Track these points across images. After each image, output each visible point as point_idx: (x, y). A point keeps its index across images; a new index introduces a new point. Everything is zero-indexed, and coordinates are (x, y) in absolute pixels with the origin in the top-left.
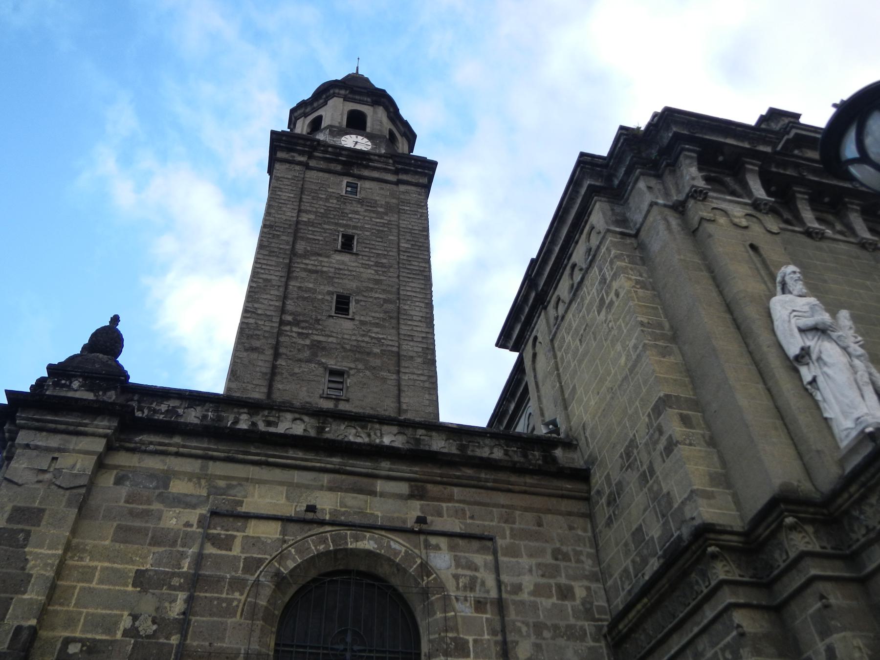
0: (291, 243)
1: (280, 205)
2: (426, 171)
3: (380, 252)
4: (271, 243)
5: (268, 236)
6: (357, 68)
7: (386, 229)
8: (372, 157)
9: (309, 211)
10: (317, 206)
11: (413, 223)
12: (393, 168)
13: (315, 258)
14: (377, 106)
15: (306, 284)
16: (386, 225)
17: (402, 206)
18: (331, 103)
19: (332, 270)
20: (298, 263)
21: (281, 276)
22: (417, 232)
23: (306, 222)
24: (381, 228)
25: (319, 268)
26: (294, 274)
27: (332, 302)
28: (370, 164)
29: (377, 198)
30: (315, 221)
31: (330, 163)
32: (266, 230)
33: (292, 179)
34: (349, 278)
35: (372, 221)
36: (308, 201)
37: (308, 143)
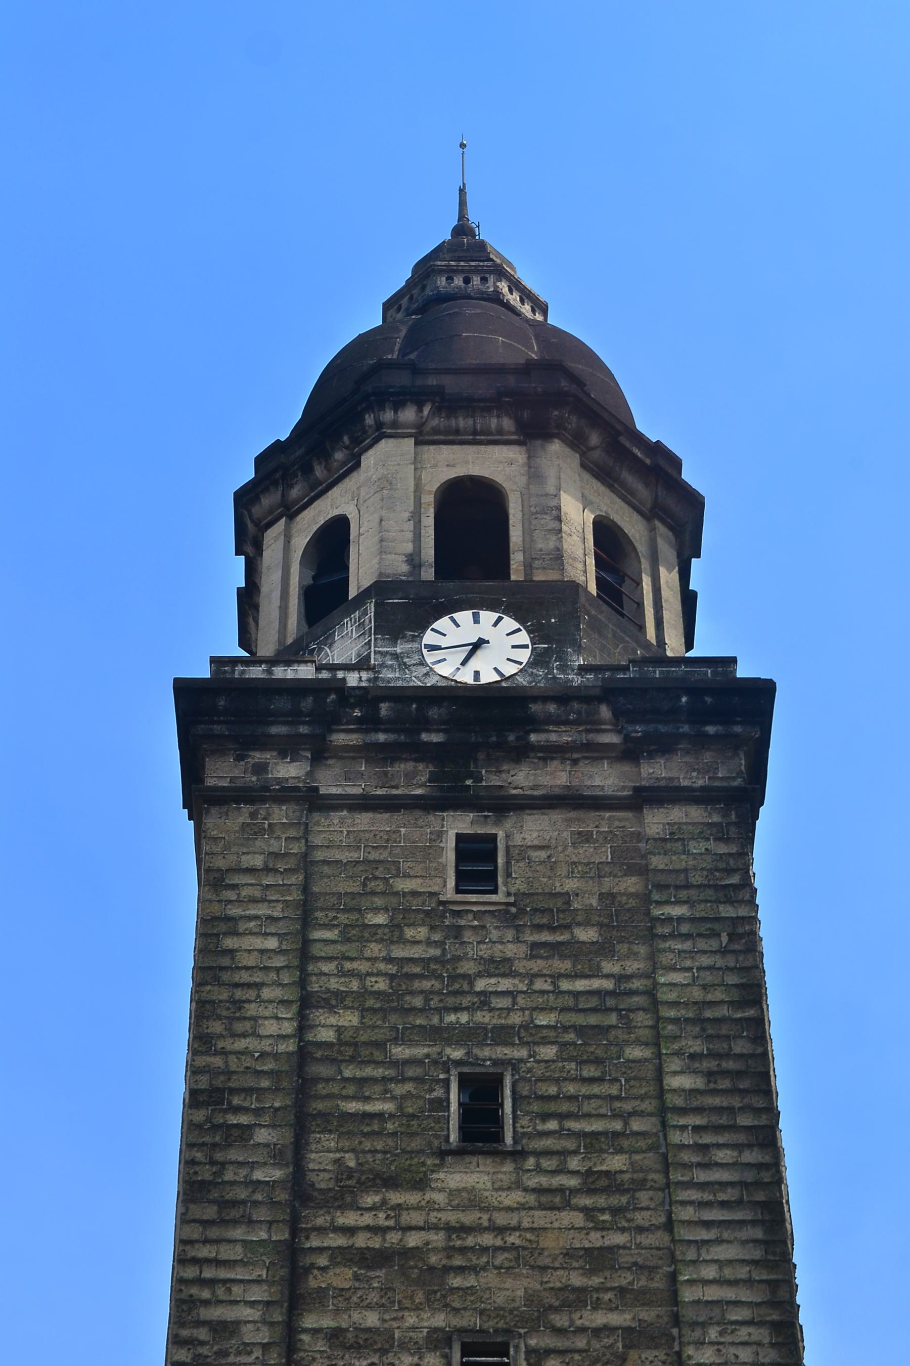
0: (289, 1155)
1: (239, 994)
2: (738, 729)
3: (596, 1126)
4: (223, 1164)
5: (207, 1139)
6: (462, 192)
7: (613, 1019)
8: (535, 708)
9: (337, 994)
10: (362, 967)
11: (707, 977)
12: (612, 738)
13: (377, 1199)
14: (539, 442)
15: (356, 1316)
16: (610, 1002)
17: (659, 903)
18: (369, 459)
19: (437, 1239)
20: (321, 1230)
21: (268, 1304)
22: (724, 1011)
23: (329, 1045)
24: (593, 1020)
25: (393, 1238)
26: (314, 1282)
28: (533, 737)
29: (571, 885)
30: (364, 1037)
31: (394, 760)
32: (200, 1116)
33: (267, 870)
34: (500, 1259)
35: (559, 993)
36: (330, 950)
37: (307, 703)
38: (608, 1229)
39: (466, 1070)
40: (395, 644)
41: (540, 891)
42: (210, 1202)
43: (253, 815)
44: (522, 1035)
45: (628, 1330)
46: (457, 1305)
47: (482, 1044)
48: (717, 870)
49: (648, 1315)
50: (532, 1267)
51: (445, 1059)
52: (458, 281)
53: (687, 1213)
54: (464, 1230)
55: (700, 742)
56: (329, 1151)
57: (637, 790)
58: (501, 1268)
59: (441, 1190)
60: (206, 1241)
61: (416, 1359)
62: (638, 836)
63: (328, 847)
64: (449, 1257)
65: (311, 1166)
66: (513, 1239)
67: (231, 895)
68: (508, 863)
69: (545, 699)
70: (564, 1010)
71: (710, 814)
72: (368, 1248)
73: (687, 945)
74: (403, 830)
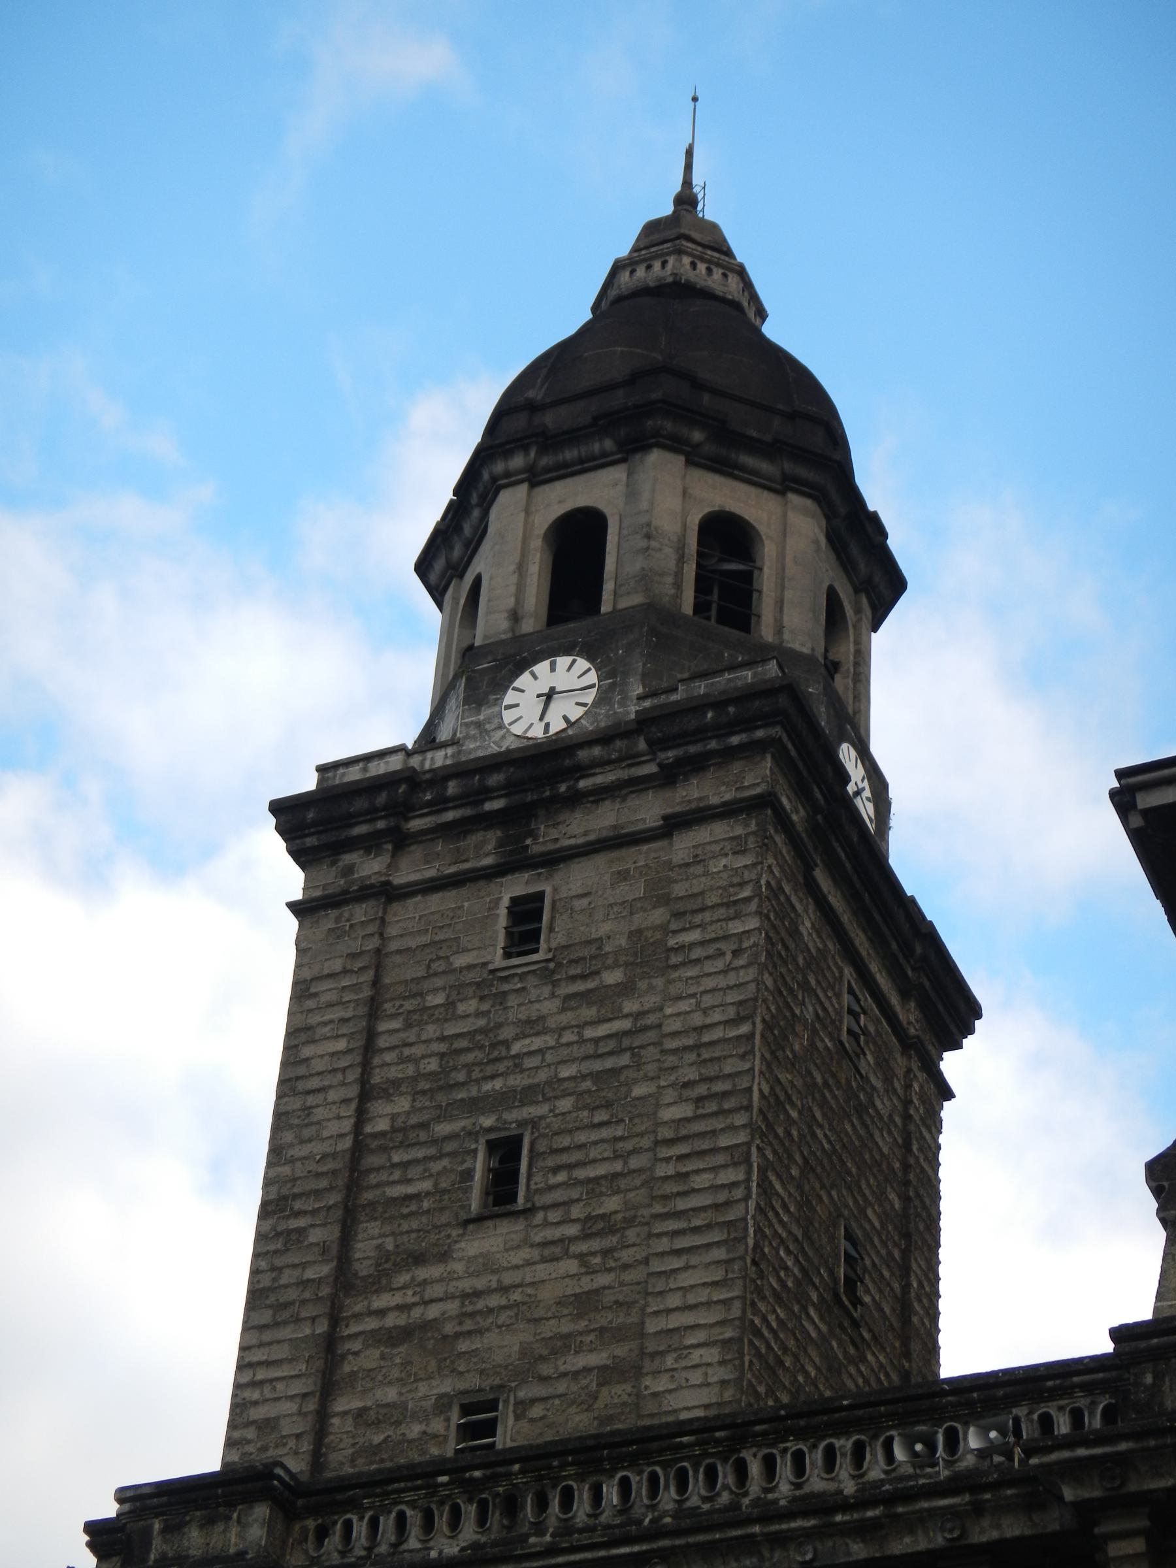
1: (311, 1100)
2: (760, 734)
3: (601, 1170)
4: (280, 1269)
6: (689, 153)
7: (625, 1059)
8: (583, 755)
10: (418, 1051)
11: (708, 1001)
12: (651, 769)
14: (638, 456)
16: (626, 1042)
19: (452, 1307)
20: (357, 1316)
21: (305, 1396)
22: (717, 1034)
23: (383, 1134)
24: (609, 1063)
25: (416, 1313)
26: (347, 1368)
27: (446, 1437)
28: (582, 784)
29: (606, 928)
30: (414, 1120)
31: (467, 833)
33: (345, 972)
34: (503, 1318)
35: (582, 1041)
37: (382, 799)
38: (597, 1272)
39: (493, 1136)
40: (479, 712)
41: (577, 941)
42: (270, 1306)
43: (337, 920)
44: (546, 1091)
45: (603, 1369)
46: (461, 1369)
47: (510, 1108)
48: (733, 886)
49: (621, 1351)
50: (529, 1321)
51: (478, 1128)
52: (641, 272)
53: (664, 1244)
54: (477, 1294)
55: (730, 754)
56: (373, 1238)
57: (665, 818)
58: (503, 1326)
59: (460, 1260)
60: (261, 1345)
61: (423, 1427)
62: (670, 866)
63: (401, 936)
64: (460, 1323)
65: (357, 1255)
66: (516, 1296)
67: (311, 1004)
68: (553, 918)
69: (589, 743)
70: (587, 1058)
71: (732, 827)
72: (395, 1327)
73: (691, 972)
74: (466, 904)
